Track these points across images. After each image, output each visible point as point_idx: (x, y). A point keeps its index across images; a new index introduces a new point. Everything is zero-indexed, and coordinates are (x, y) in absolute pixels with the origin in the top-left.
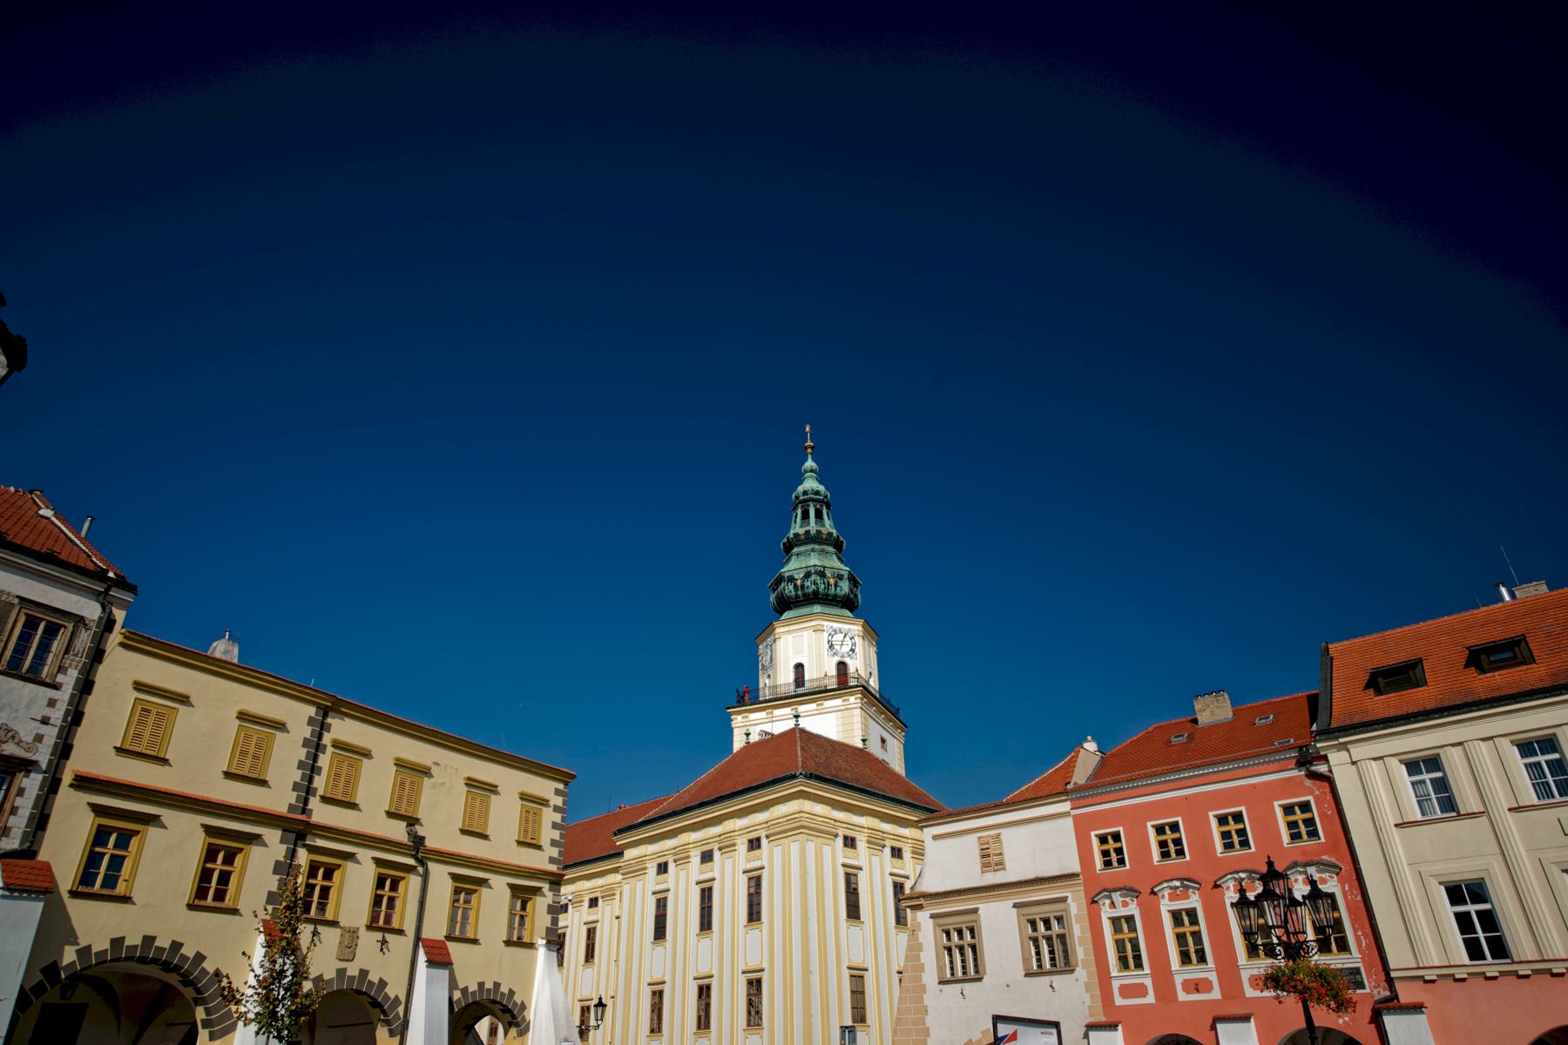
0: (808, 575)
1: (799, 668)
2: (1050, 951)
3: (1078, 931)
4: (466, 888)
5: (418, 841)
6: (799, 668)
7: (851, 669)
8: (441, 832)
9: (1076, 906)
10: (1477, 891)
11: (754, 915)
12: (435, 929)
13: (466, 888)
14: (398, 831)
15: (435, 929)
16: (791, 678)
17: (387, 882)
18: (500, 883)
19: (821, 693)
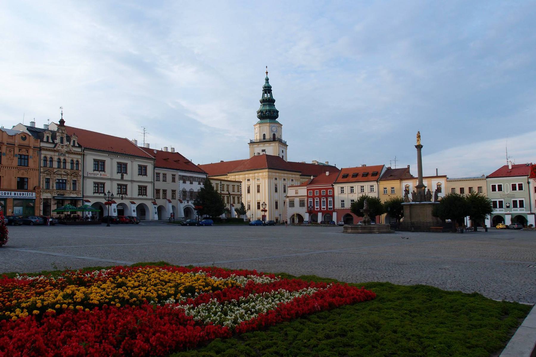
0: (266, 111)
1: (264, 135)
2: (302, 204)
3: (306, 202)
4: (234, 198)
5: (229, 193)
6: (264, 135)
7: (276, 137)
8: (231, 193)
9: (306, 199)
10: (344, 201)
11: (258, 191)
12: (232, 203)
13: (234, 198)
14: (227, 193)
15: (232, 203)
16: (262, 138)
17: (228, 198)
18: (236, 196)
19: (269, 141)
